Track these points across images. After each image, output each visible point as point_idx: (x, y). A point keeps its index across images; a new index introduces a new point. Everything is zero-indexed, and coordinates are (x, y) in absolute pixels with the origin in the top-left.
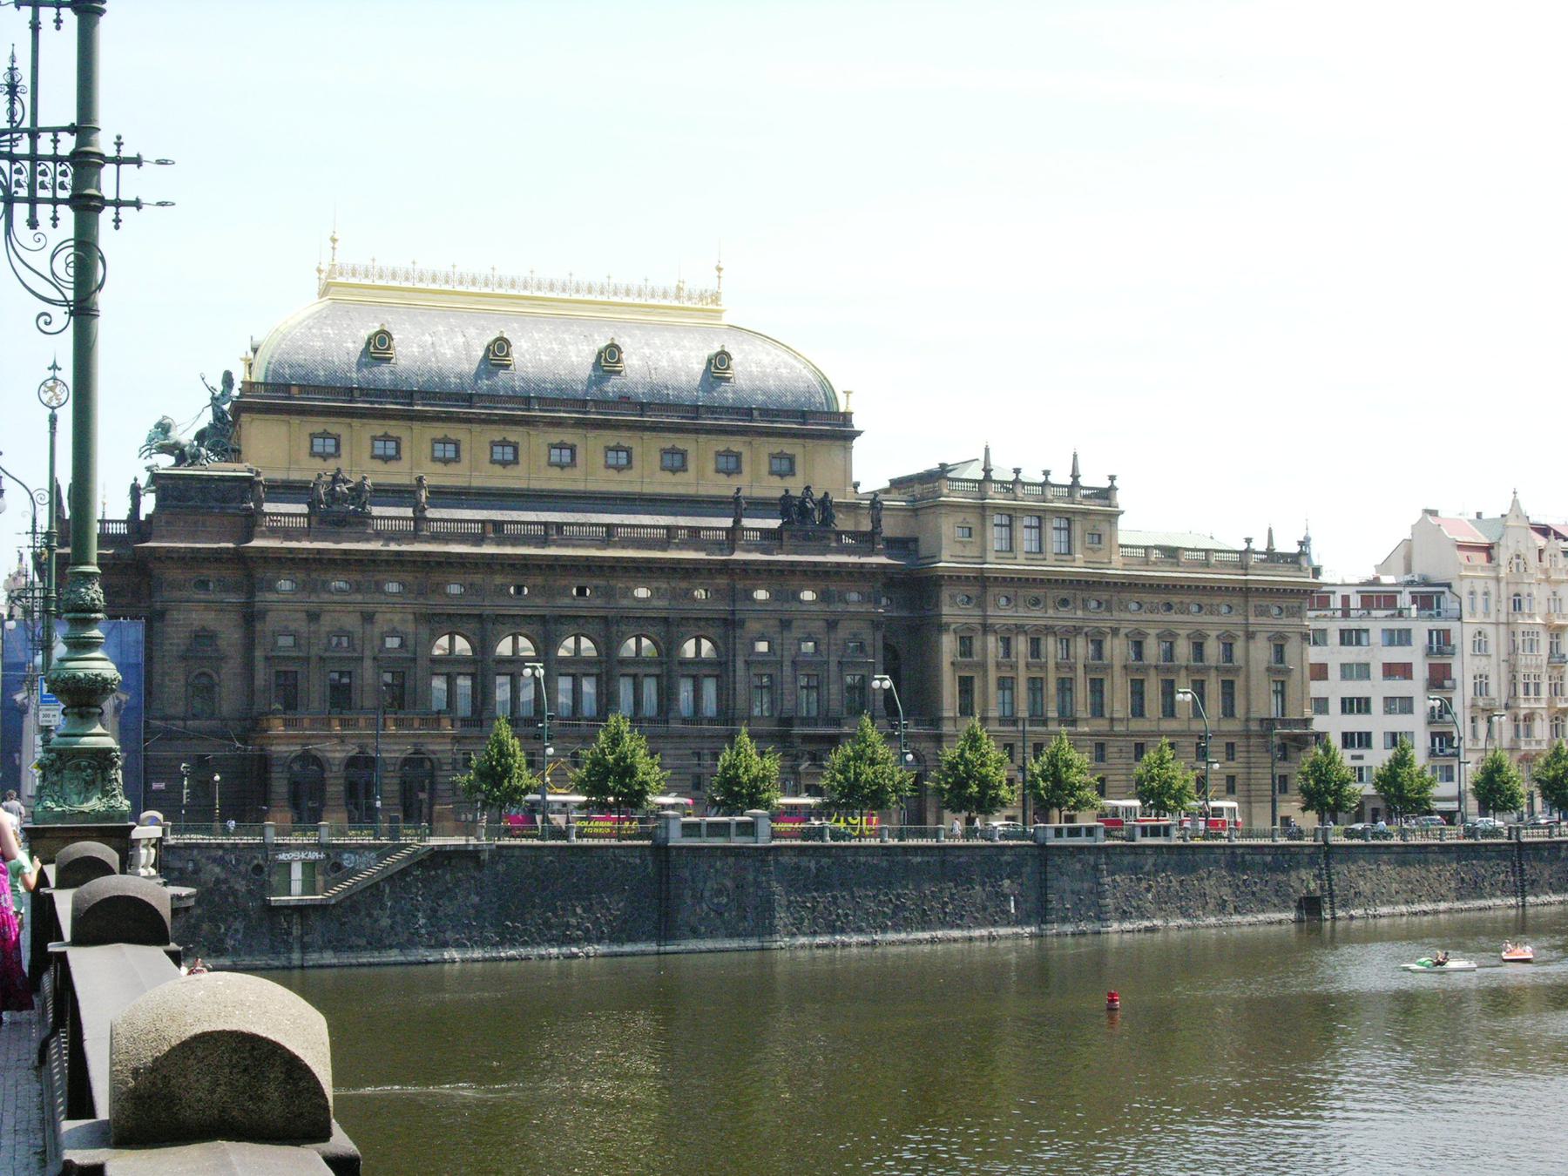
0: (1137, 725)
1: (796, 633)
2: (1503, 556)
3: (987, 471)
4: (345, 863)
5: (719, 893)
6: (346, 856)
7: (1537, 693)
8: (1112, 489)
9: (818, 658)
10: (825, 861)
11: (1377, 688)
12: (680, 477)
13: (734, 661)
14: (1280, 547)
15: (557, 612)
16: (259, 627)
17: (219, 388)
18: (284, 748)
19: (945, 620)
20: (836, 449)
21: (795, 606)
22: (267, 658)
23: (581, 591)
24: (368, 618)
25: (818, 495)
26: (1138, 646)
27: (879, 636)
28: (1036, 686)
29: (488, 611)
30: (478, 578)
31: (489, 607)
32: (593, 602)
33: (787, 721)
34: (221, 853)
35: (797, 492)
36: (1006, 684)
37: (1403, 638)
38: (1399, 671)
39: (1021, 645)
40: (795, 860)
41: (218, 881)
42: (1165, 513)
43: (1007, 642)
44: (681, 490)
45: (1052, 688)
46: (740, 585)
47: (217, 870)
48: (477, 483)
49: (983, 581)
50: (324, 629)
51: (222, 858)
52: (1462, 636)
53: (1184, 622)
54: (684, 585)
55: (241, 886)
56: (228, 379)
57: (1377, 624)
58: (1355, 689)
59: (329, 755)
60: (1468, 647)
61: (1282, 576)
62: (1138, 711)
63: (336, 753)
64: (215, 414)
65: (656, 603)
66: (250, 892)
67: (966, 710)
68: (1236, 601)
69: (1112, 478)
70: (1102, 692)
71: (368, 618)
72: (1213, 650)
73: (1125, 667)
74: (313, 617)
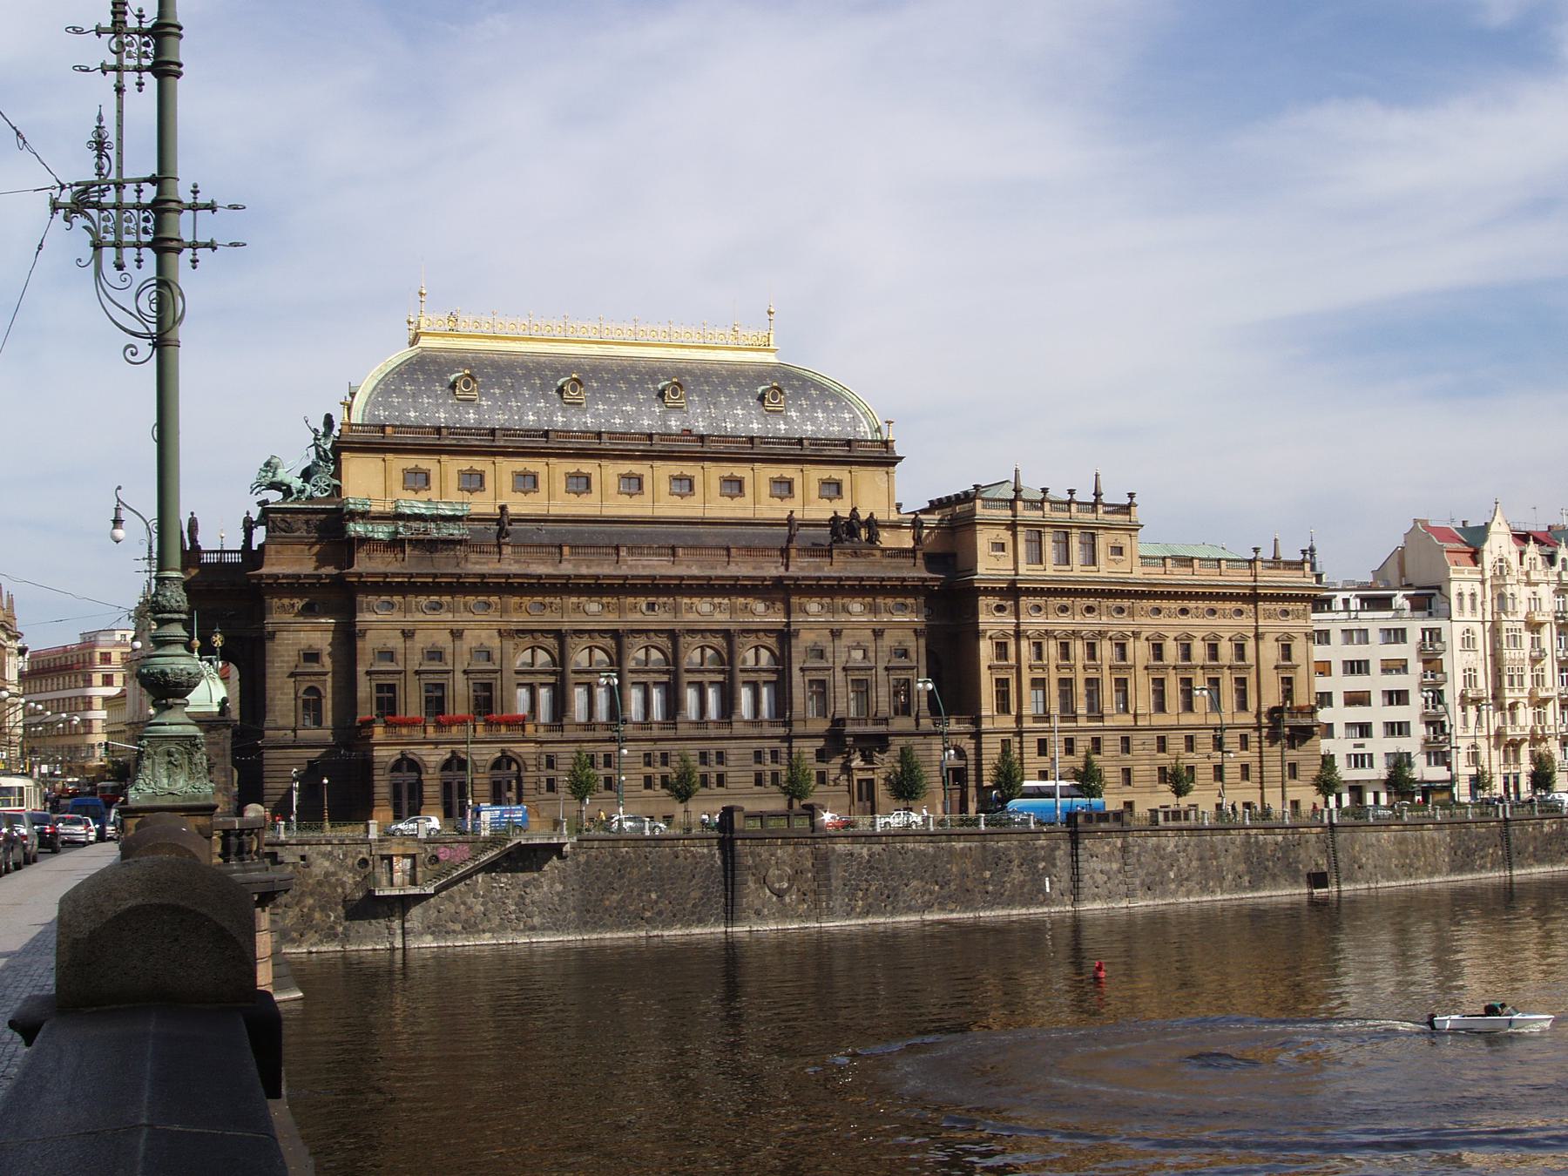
2: (1488, 558)
3: (1017, 490)
4: (441, 856)
5: (780, 879)
7: (1521, 683)
9: (867, 664)
10: (877, 848)
11: (1375, 683)
14: (1285, 556)
15: (629, 627)
16: (360, 644)
17: (322, 430)
19: (981, 627)
20: (878, 473)
21: (843, 617)
23: (651, 606)
24: (456, 634)
25: (864, 516)
27: (922, 642)
28: (1066, 684)
29: (566, 627)
32: (662, 617)
33: (838, 722)
34: (329, 848)
35: (845, 513)
37: (1399, 635)
38: (1395, 667)
40: (849, 847)
41: (327, 874)
43: (1039, 646)
44: (740, 514)
45: (1080, 689)
46: (794, 600)
47: (327, 864)
48: (554, 511)
49: (1012, 592)
51: (331, 853)
52: (1453, 632)
53: (1198, 624)
56: (329, 422)
57: (1375, 621)
58: (1357, 683)
60: (1457, 645)
62: (1160, 707)
63: (433, 757)
64: (318, 453)
65: (718, 616)
66: (357, 884)
67: (1003, 707)
69: (1131, 495)
70: (1126, 691)
71: (456, 634)
72: (1226, 651)
73: (1146, 668)
74: (407, 635)
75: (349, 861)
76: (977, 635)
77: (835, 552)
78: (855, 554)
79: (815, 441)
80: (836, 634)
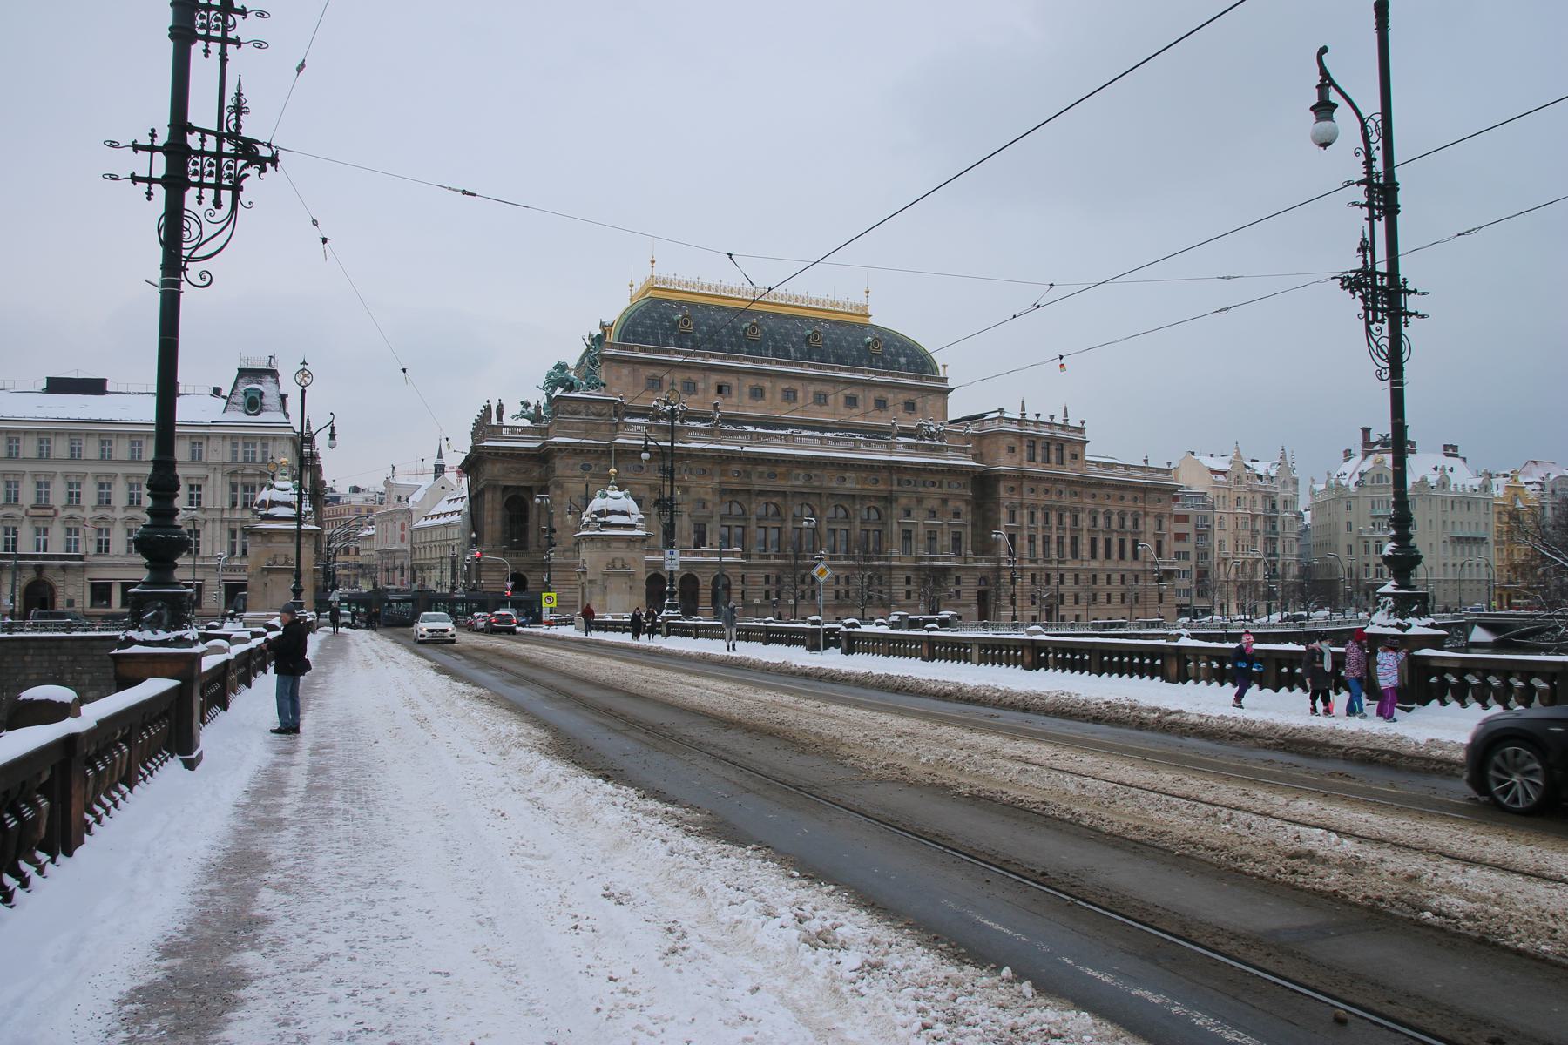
0: (1095, 564)
8: (1081, 430)
26: (1095, 519)
28: (1046, 540)
36: (1032, 539)
39: (1039, 515)
42: (1112, 445)
61: (1159, 479)
62: (1094, 556)
65: (848, 485)
68: (1140, 495)
72: (1129, 523)
76: (998, 505)
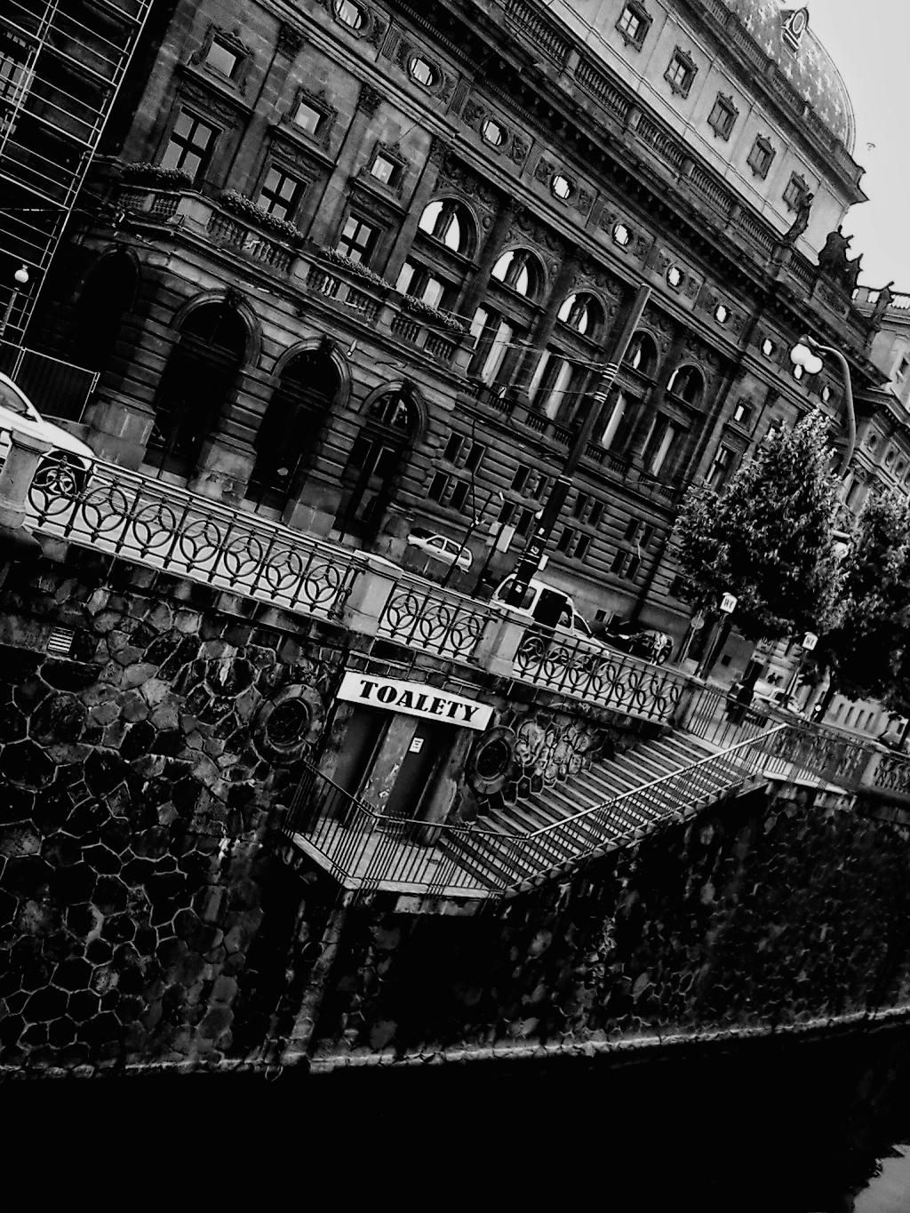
1: (773, 413)
6: (532, 728)
12: (717, 143)
13: (714, 420)
18: (193, 276)
22: (179, 71)
24: (369, 101)
30: (527, 135)
31: (526, 187)
46: (763, 324)
47: (155, 690)
50: (296, 77)
54: (714, 292)
55: (214, 772)
59: (269, 331)
63: (280, 332)
66: (240, 797)
71: (369, 101)
75: (246, 702)
77: (819, 283)
78: (832, 301)
79: (812, 114)
80: (772, 396)
